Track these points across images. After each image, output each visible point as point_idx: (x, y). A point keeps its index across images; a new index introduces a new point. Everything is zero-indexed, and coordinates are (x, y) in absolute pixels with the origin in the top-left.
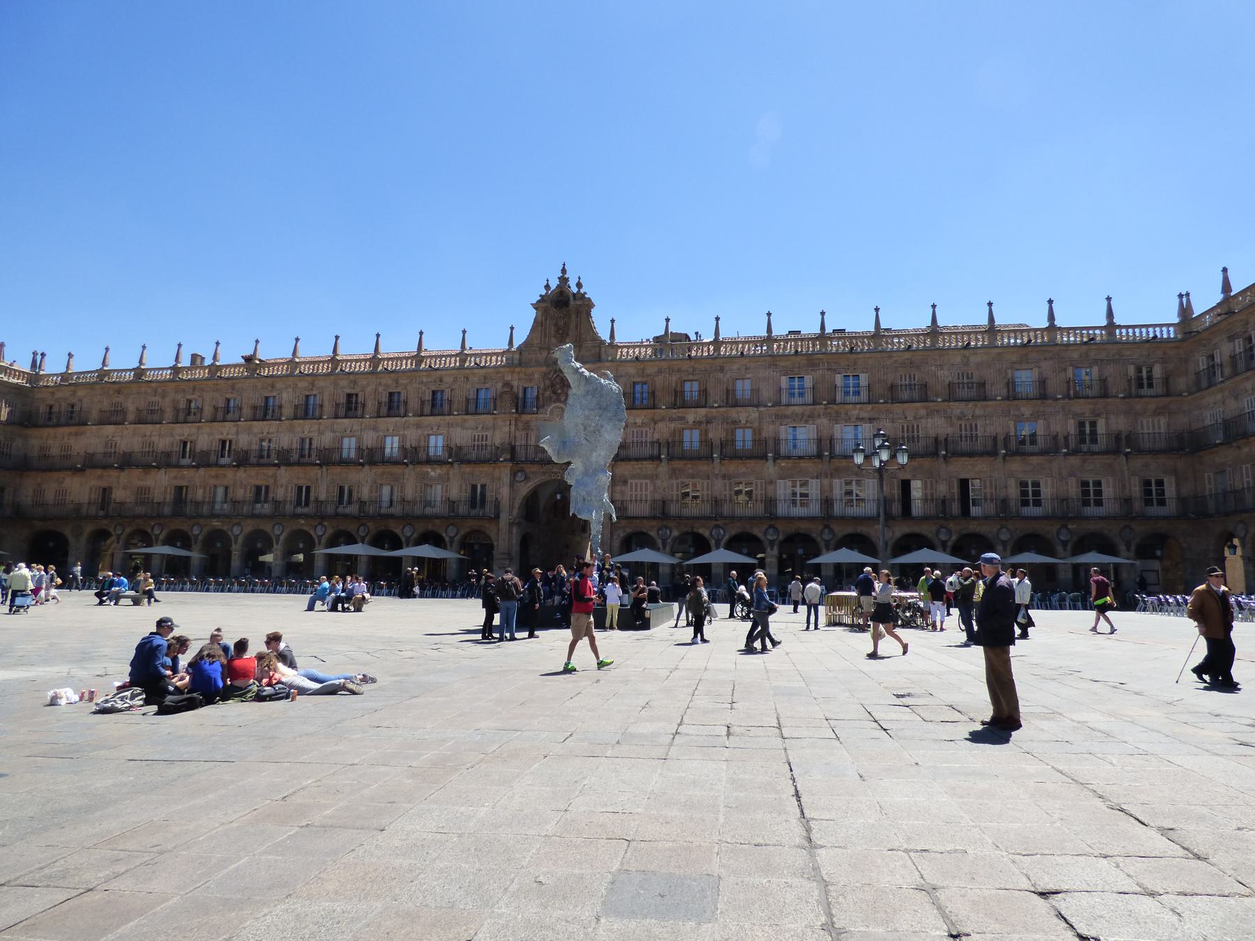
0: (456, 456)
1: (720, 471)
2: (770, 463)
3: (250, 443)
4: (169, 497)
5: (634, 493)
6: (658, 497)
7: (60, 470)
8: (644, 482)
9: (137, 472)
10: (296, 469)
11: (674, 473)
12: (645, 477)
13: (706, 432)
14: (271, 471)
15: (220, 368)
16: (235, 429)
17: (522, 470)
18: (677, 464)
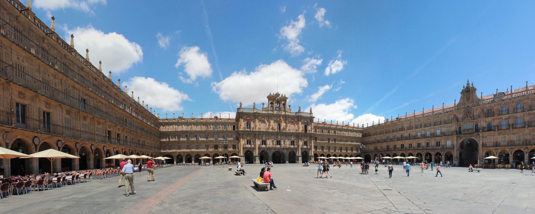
0: (443, 134)
1: (512, 132)
2: (527, 128)
3: (399, 136)
4: (386, 148)
5: (488, 140)
6: (495, 141)
7: (368, 144)
8: (491, 137)
9: (380, 143)
10: (409, 140)
11: (499, 134)
12: (491, 136)
13: (508, 121)
14: (404, 141)
15: (393, 121)
16: (396, 133)
17: (459, 136)
18: (500, 131)
